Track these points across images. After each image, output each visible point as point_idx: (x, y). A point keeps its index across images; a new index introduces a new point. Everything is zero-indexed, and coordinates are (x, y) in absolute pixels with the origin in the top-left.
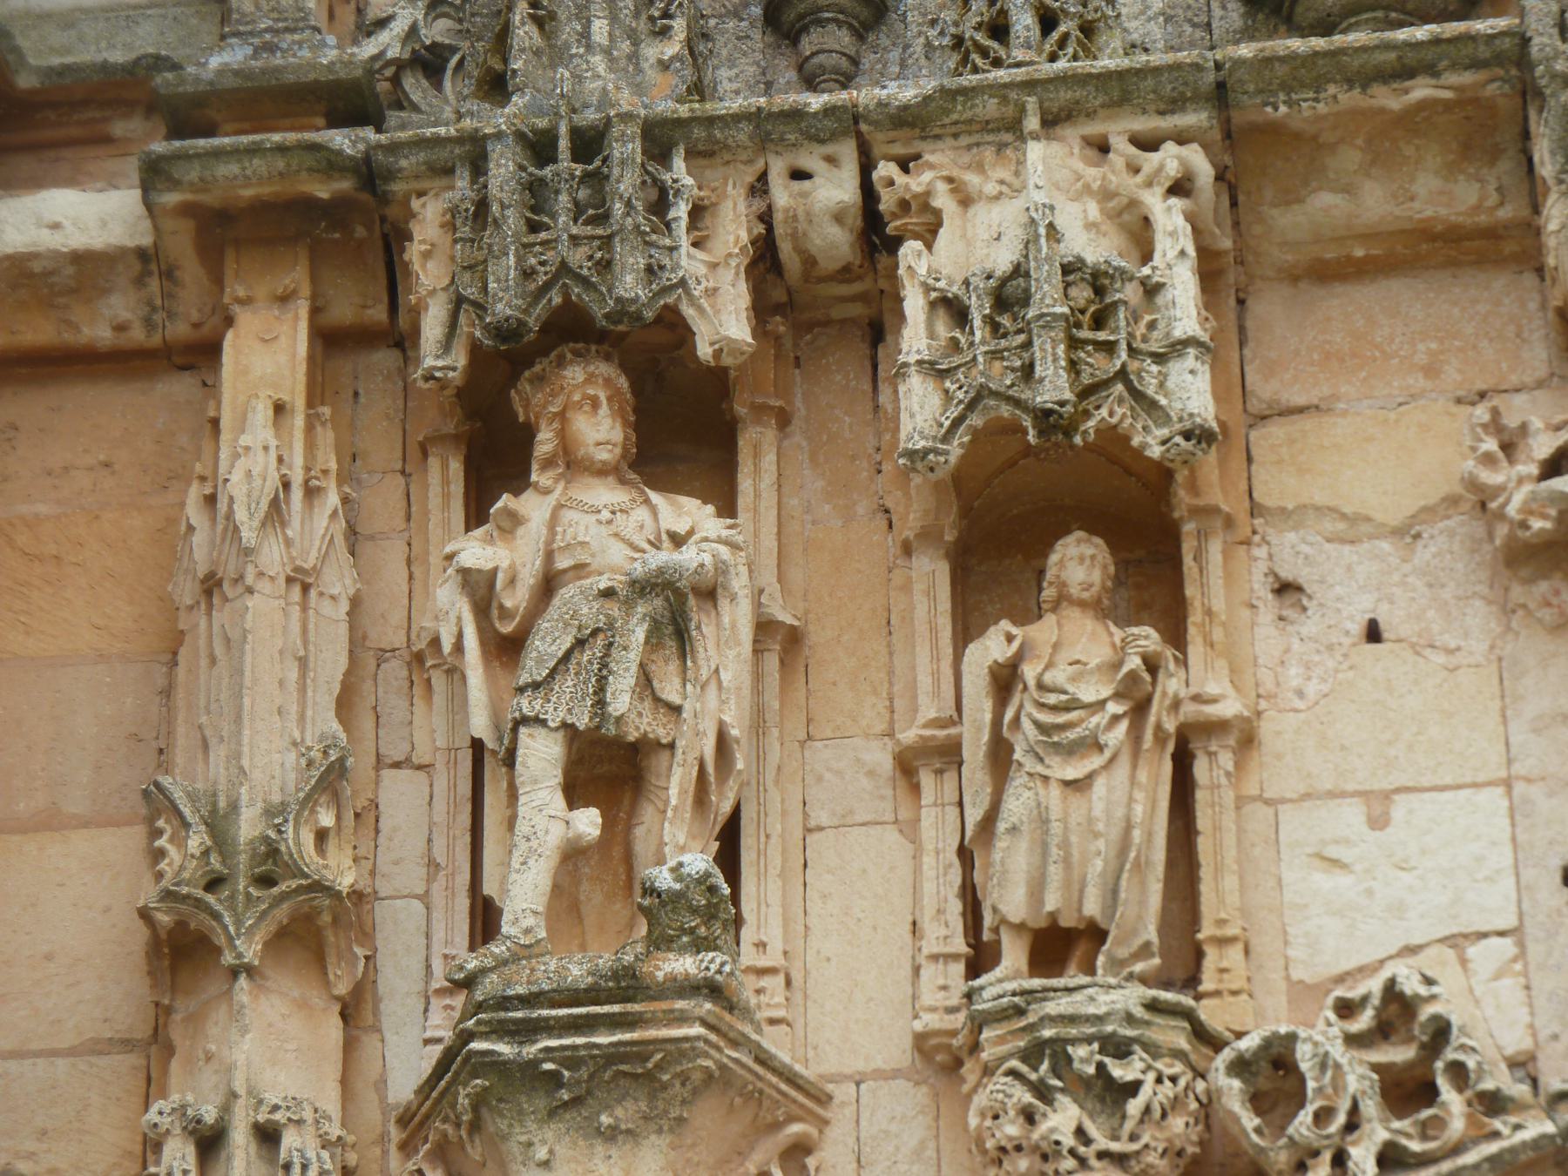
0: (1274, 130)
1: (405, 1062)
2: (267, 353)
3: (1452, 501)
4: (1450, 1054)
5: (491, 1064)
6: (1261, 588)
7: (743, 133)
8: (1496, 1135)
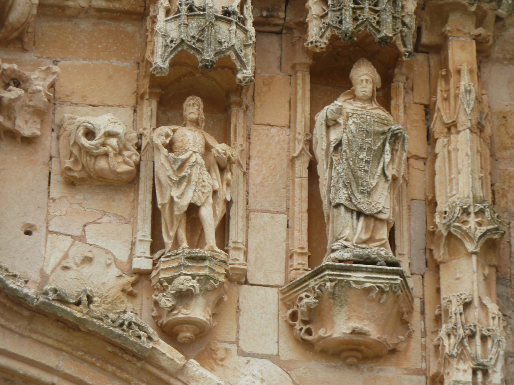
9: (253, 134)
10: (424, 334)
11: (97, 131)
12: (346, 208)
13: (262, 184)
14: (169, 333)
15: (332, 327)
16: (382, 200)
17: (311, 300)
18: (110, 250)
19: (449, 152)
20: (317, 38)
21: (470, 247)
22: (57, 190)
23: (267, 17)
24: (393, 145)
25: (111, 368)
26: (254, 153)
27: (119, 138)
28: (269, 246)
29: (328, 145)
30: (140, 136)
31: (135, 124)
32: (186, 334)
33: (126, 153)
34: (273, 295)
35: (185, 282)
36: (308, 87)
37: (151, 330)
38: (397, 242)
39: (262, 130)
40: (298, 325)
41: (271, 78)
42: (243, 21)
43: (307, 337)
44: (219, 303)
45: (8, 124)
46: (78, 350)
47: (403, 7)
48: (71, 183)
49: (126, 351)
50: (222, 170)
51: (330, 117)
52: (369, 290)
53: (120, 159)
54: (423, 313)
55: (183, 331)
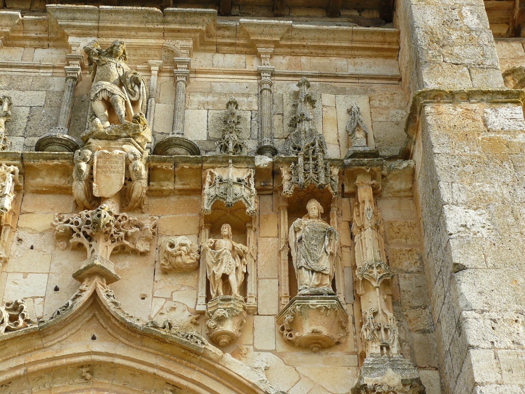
0: (31, 167)
3: (51, 229)
4: (22, 312)
6: (15, 239)
8: (27, 327)
9: (259, 242)
10: (355, 333)
11: (175, 244)
12: (305, 268)
13: (264, 266)
14: (215, 341)
15: (302, 331)
16: (325, 264)
17: (290, 317)
18: (185, 303)
19: (361, 240)
20: (287, 190)
21: (375, 284)
23: (264, 186)
25: (184, 362)
26: (260, 251)
27: (187, 246)
28: (268, 294)
29: (296, 241)
30: (200, 247)
31: (198, 242)
32: (224, 340)
33: (191, 254)
34: (272, 319)
35: (220, 312)
36: (287, 217)
37: (204, 339)
38: (337, 288)
39: (264, 240)
40: (285, 333)
41: (268, 215)
42: (250, 185)
43: (290, 338)
44: (242, 324)
45: (132, 246)
46: (167, 354)
47: (331, 173)
48: (165, 272)
49: (191, 351)
50: (241, 258)
51: (296, 226)
52: (319, 309)
53: (189, 257)
54: (354, 323)
55: (221, 339)
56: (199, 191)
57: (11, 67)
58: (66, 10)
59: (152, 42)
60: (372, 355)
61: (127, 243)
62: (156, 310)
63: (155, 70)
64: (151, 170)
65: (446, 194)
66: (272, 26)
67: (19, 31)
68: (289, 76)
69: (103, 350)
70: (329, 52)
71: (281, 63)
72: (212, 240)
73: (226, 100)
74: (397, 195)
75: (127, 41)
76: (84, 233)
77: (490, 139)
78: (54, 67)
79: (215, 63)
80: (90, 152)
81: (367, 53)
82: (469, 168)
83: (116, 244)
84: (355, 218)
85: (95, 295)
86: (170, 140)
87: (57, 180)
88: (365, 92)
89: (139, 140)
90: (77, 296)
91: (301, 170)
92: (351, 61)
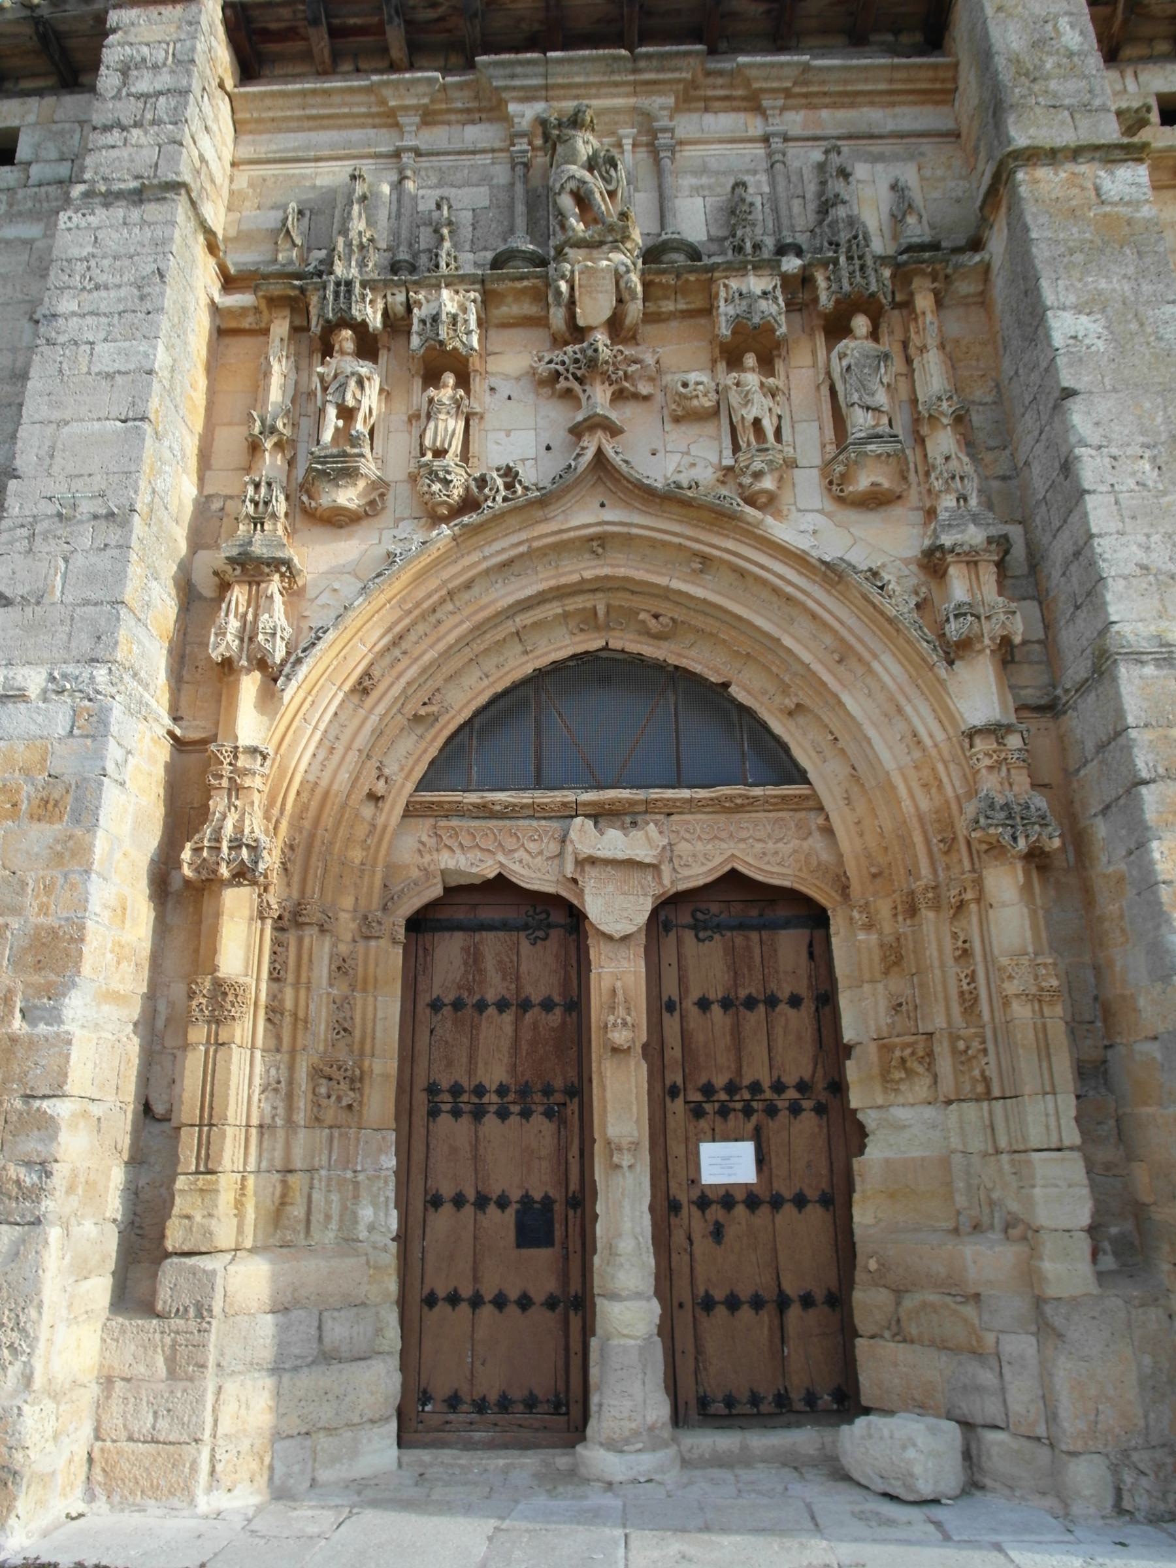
0: (494, 291)
1: (300, 472)
2: (280, 328)
5: (317, 470)
6: (487, 388)
7: (381, 285)
10: (919, 484)
14: (751, 501)
16: (881, 398)
21: (945, 421)
22: (668, 427)
24: (885, 361)
28: (808, 441)
31: (713, 379)
32: (763, 500)
34: (815, 472)
35: (757, 465)
40: (834, 487)
42: (776, 298)
44: (781, 479)
45: (632, 389)
48: (677, 420)
50: (773, 396)
52: (879, 456)
56: (708, 311)
57: (438, 154)
58: (502, 64)
59: (620, 102)
60: (946, 509)
61: (627, 385)
62: (671, 468)
63: (627, 143)
64: (646, 285)
65: (1049, 297)
66: (782, 65)
67: (441, 101)
68: (807, 139)
69: (616, 519)
70: (859, 99)
71: (795, 121)
72: (735, 374)
73: (731, 181)
74: (964, 302)
75: (595, 103)
76: (573, 374)
77: (1105, 215)
78: (493, 151)
79: (706, 128)
80: (568, 267)
81: (911, 98)
82: (1079, 258)
83: (615, 387)
84: (913, 335)
85: (600, 452)
86: (665, 242)
87: (528, 308)
88: (911, 157)
89: (629, 245)
90: (579, 455)
91: (845, 274)
92: (889, 111)
